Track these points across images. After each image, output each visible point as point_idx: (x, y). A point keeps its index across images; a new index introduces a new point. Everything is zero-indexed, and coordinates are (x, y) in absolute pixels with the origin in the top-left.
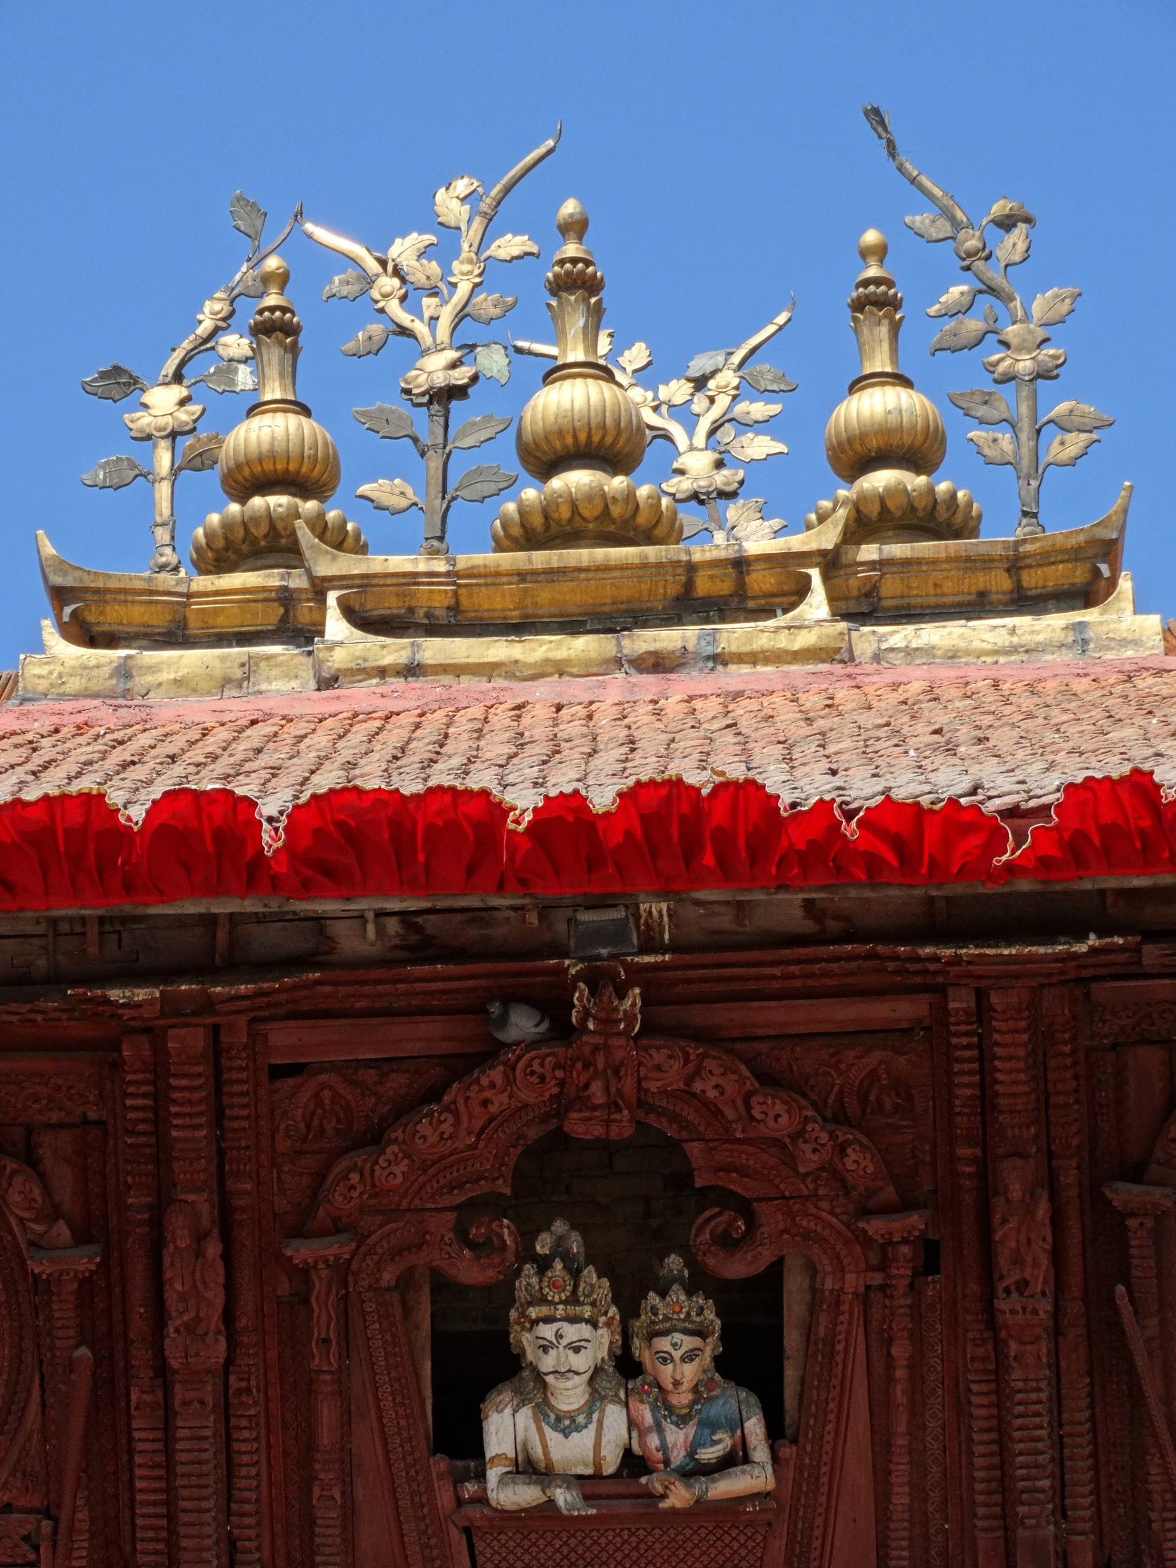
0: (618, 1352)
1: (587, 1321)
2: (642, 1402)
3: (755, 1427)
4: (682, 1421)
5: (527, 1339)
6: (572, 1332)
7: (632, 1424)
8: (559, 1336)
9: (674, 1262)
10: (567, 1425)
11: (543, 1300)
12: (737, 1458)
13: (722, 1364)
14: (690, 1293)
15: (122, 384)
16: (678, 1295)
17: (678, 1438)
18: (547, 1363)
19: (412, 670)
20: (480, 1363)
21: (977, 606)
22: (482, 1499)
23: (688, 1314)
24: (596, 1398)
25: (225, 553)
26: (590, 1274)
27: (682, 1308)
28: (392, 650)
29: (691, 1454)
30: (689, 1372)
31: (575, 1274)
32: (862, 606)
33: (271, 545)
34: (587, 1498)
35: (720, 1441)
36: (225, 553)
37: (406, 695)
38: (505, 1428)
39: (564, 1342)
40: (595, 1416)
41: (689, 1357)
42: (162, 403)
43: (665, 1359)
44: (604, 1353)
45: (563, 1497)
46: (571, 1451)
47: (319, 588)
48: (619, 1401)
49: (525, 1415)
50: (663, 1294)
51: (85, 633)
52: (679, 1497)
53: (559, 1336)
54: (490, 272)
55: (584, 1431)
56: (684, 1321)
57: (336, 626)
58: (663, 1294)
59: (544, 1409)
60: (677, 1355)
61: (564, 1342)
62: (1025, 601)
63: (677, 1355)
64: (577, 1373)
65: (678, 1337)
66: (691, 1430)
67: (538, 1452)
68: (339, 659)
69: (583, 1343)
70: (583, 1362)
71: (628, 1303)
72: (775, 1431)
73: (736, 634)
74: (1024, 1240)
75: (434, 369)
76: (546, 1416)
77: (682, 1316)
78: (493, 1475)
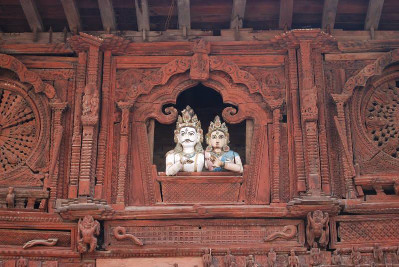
0: (202, 141)
1: (194, 127)
2: (208, 152)
3: (238, 158)
6: (191, 130)
8: (186, 130)
20: (165, 139)
23: (221, 127)
40: (195, 155)
41: (221, 137)
43: (214, 137)
44: (198, 140)
53: (186, 130)
60: (218, 136)
64: (191, 141)
65: (218, 131)
72: (244, 162)
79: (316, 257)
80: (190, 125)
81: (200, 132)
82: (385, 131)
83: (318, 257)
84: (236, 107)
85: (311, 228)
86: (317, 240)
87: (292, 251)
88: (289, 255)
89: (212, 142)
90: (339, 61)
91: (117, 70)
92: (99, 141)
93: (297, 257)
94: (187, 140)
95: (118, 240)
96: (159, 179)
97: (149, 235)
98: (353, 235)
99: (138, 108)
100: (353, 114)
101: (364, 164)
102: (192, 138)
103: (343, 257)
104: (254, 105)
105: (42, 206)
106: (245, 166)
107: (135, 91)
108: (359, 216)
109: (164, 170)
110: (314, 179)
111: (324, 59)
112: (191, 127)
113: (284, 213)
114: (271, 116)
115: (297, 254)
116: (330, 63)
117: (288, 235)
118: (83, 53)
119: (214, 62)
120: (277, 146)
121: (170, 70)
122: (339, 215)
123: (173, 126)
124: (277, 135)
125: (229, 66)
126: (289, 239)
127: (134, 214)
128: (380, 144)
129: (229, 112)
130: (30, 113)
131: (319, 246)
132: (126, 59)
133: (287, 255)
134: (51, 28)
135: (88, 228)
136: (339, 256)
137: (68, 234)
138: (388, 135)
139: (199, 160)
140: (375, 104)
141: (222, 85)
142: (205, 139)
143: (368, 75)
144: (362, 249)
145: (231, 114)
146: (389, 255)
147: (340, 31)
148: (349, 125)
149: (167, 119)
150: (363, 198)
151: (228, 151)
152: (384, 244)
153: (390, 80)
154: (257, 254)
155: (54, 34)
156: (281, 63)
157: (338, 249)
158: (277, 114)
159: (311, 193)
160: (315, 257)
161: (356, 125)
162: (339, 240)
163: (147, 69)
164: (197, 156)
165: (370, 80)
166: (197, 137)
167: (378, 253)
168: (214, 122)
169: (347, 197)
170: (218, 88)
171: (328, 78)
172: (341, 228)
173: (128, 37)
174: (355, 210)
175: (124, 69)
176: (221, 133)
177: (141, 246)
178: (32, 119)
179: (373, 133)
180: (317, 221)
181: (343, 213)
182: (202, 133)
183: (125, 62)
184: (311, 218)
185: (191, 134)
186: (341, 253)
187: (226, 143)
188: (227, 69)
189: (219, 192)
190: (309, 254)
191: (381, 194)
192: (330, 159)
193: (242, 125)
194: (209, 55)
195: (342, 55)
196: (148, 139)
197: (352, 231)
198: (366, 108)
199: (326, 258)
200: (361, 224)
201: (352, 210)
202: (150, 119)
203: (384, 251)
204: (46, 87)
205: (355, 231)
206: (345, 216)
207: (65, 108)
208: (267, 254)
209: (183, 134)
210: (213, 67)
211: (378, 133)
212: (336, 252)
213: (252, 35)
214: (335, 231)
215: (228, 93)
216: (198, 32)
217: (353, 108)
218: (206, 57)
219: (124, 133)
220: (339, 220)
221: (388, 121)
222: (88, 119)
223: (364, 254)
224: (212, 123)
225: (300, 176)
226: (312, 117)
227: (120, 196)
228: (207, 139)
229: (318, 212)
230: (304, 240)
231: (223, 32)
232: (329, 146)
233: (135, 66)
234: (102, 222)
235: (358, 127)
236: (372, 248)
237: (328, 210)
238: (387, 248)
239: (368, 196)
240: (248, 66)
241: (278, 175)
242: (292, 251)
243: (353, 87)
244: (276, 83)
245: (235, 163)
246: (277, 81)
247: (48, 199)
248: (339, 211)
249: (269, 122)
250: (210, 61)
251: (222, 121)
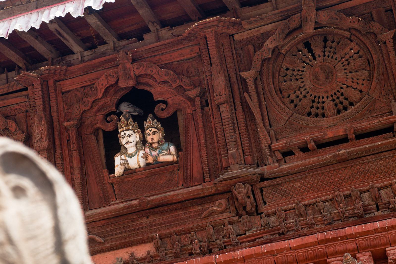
0: (142, 139)
2: (147, 148)
4: (155, 149)
6: (128, 133)
8: (125, 134)
23: (153, 124)
24: (138, 150)
27: (151, 122)
35: (164, 152)
39: (126, 135)
40: (137, 153)
41: (154, 133)
43: (148, 135)
44: (138, 139)
48: (143, 150)
53: (125, 134)
55: (135, 156)
56: (152, 125)
60: (151, 133)
61: (126, 135)
63: (151, 133)
64: (131, 143)
65: (150, 129)
69: (130, 135)
72: (178, 149)
76: (126, 155)
77: (151, 124)
79: (246, 223)
80: (127, 128)
81: (138, 132)
82: (298, 93)
83: (247, 223)
84: (165, 102)
85: (237, 199)
86: (244, 208)
87: (226, 222)
88: (224, 226)
89: (149, 139)
90: (248, 38)
91: (63, 93)
92: (56, 160)
93: (230, 226)
94: (127, 142)
96: (110, 182)
97: (108, 232)
98: (276, 197)
99: (84, 123)
100: (266, 85)
101: (280, 129)
102: (131, 139)
103: (270, 218)
104: (179, 98)
107: (78, 110)
108: (278, 180)
109: (113, 172)
110: (232, 155)
111: (234, 39)
112: (129, 130)
113: (213, 190)
114: (194, 105)
115: (230, 223)
116: (240, 42)
117: (219, 209)
118: (31, 87)
119: (137, 68)
120: (201, 131)
121: (102, 84)
122: (260, 182)
123: (116, 132)
124: (200, 121)
125: (150, 69)
126: (222, 212)
127: (91, 218)
128: (296, 106)
129: (160, 108)
131: (249, 214)
132: (68, 82)
133: (223, 226)
134: (6, 69)
136: (266, 218)
138: (301, 96)
140: (287, 69)
141: (151, 86)
143: (271, 46)
144: (286, 208)
145: (163, 109)
146: (311, 208)
147: (247, 9)
148: (262, 96)
149: (110, 127)
150: (283, 160)
151: (164, 144)
152: (304, 199)
153: (298, 43)
154: (198, 230)
155: (9, 74)
156: (198, 53)
157: (265, 212)
158: (198, 102)
159: (231, 169)
160: (245, 224)
161: (269, 95)
162: (265, 203)
163: (87, 86)
164: (138, 154)
165: (276, 52)
166: (136, 137)
167: (298, 209)
168: (146, 121)
169: (267, 163)
170: (148, 89)
171: (240, 56)
172: (264, 193)
173: (68, 61)
174: (278, 174)
175: (69, 92)
177: (101, 243)
180: (240, 193)
181: (263, 179)
182: (140, 132)
183: (68, 85)
184: (234, 190)
185: (129, 136)
186: (268, 215)
187: (161, 136)
188: (149, 72)
189: (162, 182)
190: (241, 221)
191: (298, 154)
192: (250, 131)
193: (174, 116)
194: (132, 63)
195: (249, 32)
196: (98, 148)
197: (275, 194)
198: (279, 75)
199: (256, 222)
200: (281, 186)
201: (270, 176)
202: (98, 129)
203: (306, 206)
204: (8, 123)
205: (278, 193)
206: (266, 182)
207: (25, 138)
208: (206, 229)
209: (123, 138)
210: (137, 73)
211: (293, 96)
212: (263, 215)
213: (170, 32)
214: (260, 196)
215: (158, 92)
216: (124, 42)
217: (265, 79)
218: (129, 65)
219: (75, 149)
220: (261, 186)
221: (299, 82)
222: (40, 145)
223: (288, 212)
224: (145, 122)
225: (224, 154)
226: (222, 100)
228: (146, 136)
229: (239, 185)
230: (235, 210)
231: (146, 36)
232: (248, 119)
233: (77, 86)
235: (271, 95)
236: (294, 205)
237: (247, 180)
238: (307, 202)
239: (287, 158)
240: (169, 63)
241: (206, 157)
242: (226, 222)
243: (260, 60)
244: (196, 72)
245: (169, 155)
246: (197, 71)
248: (259, 179)
249: (193, 110)
250: (133, 68)
251: (155, 117)
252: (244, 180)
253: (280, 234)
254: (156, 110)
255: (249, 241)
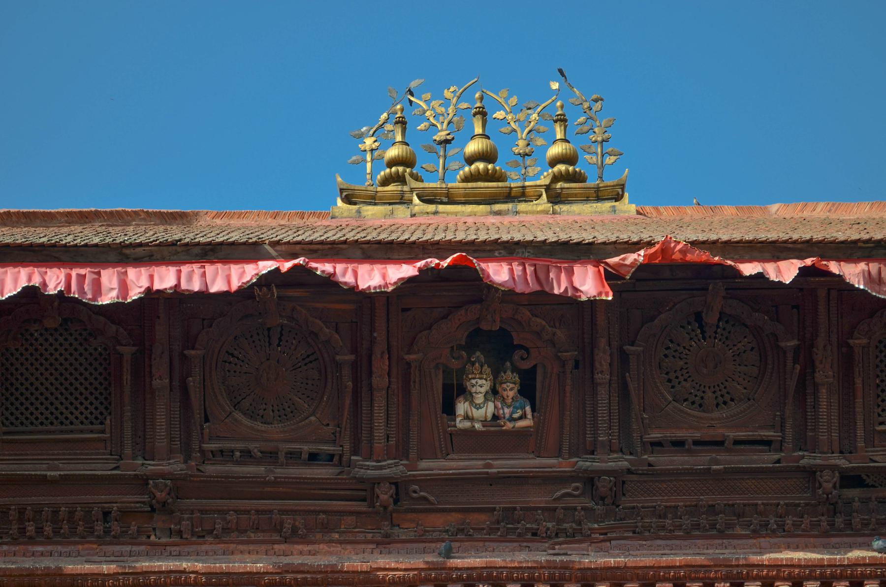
3: (528, 409)
4: (508, 407)
5: (468, 384)
6: (480, 382)
7: (495, 407)
9: (508, 364)
10: (478, 407)
11: (473, 373)
12: (523, 417)
13: (519, 392)
14: (512, 373)
15: (361, 137)
16: (509, 373)
17: (507, 411)
18: (474, 390)
19: (436, 213)
20: (454, 390)
21: (587, 199)
22: (455, 426)
24: (486, 399)
25: (385, 182)
26: (486, 367)
28: (431, 208)
29: (511, 416)
30: (511, 394)
31: (482, 366)
32: (556, 198)
33: (400, 179)
34: (484, 426)
36: (385, 182)
37: (434, 220)
38: (462, 407)
41: (511, 389)
42: (369, 142)
45: (478, 426)
46: (478, 413)
47: (412, 190)
49: (467, 404)
50: (505, 373)
51: (349, 199)
52: (510, 425)
54: (457, 112)
57: (416, 200)
58: (505, 373)
59: (472, 402)
62: (599, 199)
66: (511, 409)
67: (470, 414)
68: (416, 209)
70: (483, 390)
71: (496, 374)
72: (533, 410)
73: (522, 207)
74: (603, 359)
75: (441, 136)
78: (458, 420)
82: (679, 374)
84: (527, 350)
95: (413, 498)
105: (336, 459)
106: (535, 414)
130: (313, 354)
135: (385, 495)
137: (364, 493)
139: (490, 408)
142: (495, 385)
149: (455, 364)
158: (570, 365)
175: (409, 309)
176: (511, 385)
178: (315, 360)
179: (667, 373)
211: (672, 375)
227: (413, 454)
234: (396, 484)
247: (341, 456)
251: (515, 369)
252: (608, 472)
253: (634, 532)
254: (516, 357)
255: (601, 534)
